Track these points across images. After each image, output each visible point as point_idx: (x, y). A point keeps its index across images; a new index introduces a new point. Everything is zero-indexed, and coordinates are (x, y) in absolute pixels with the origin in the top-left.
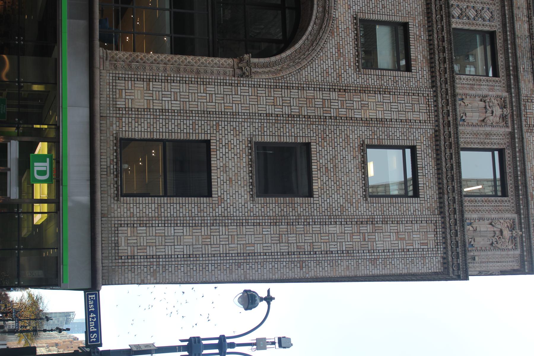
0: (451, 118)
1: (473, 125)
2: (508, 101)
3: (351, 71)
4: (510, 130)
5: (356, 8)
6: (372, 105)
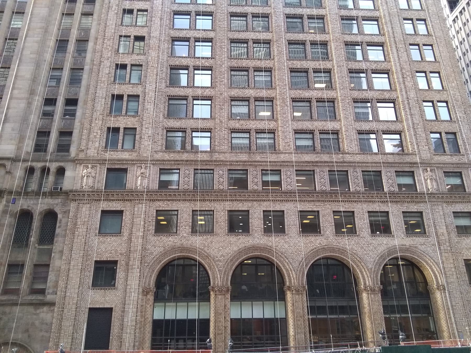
0: (440, 196)
1: (438, 185)
2: (424, 168)
3: (430, 240)
4: (436, 168)
5: (403, 235)
6: (442, 231)
